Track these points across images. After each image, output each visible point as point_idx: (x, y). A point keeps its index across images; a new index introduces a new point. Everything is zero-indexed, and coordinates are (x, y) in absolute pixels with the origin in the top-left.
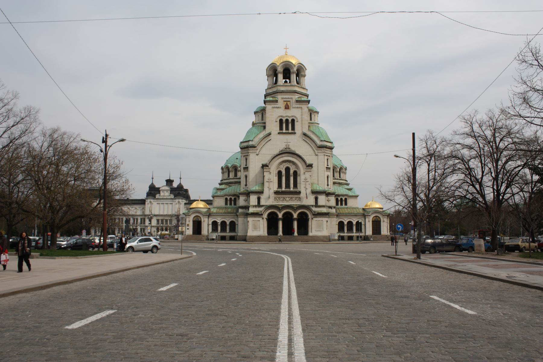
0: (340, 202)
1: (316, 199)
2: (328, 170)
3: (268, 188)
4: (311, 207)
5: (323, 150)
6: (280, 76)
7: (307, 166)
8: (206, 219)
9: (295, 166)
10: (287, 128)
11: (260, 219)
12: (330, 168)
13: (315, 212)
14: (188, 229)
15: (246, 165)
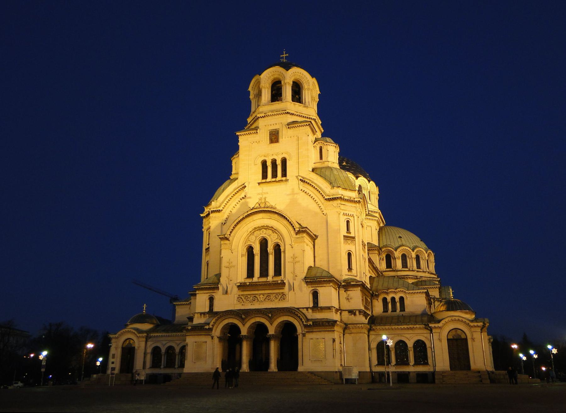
0: (390, 305)
1: (315, 295)
2: (349, 242)
3: (229, 279)
4: (304, 311)
5: (335, 203)
6: (266, 95)
7: (297, 234)
8: (143, 344)
9: (276, 235)
10: (274, 175)
11: (208, 339)
12: (354, 238)
13: (308, 320)
14: (113, 363)
15: (208, 244)
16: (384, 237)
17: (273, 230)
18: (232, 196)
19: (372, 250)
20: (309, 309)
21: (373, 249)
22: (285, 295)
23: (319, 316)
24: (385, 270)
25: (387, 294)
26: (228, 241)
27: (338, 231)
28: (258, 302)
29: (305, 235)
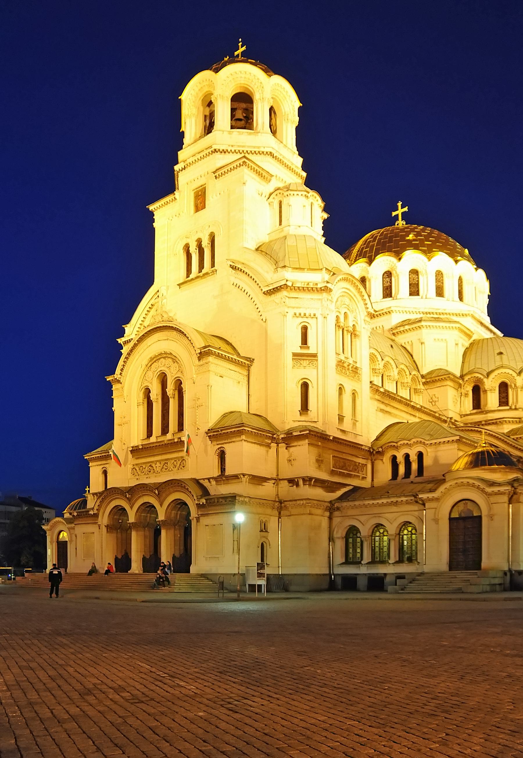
1: (222, 455)
4: (206, 483)
11: (91, 528)
16: (473, 356)
17: (173, 359)
18: (146, 314)
19: (440, 381)
20: (211, 480)
21: (442, 379)
22: (184, 460)
23: (225, 489)
24: (468, 413)
25: (397, 449)
26: (120, 384)
27: (280, 347)
28: (154, 473)
29: (211, 359)
